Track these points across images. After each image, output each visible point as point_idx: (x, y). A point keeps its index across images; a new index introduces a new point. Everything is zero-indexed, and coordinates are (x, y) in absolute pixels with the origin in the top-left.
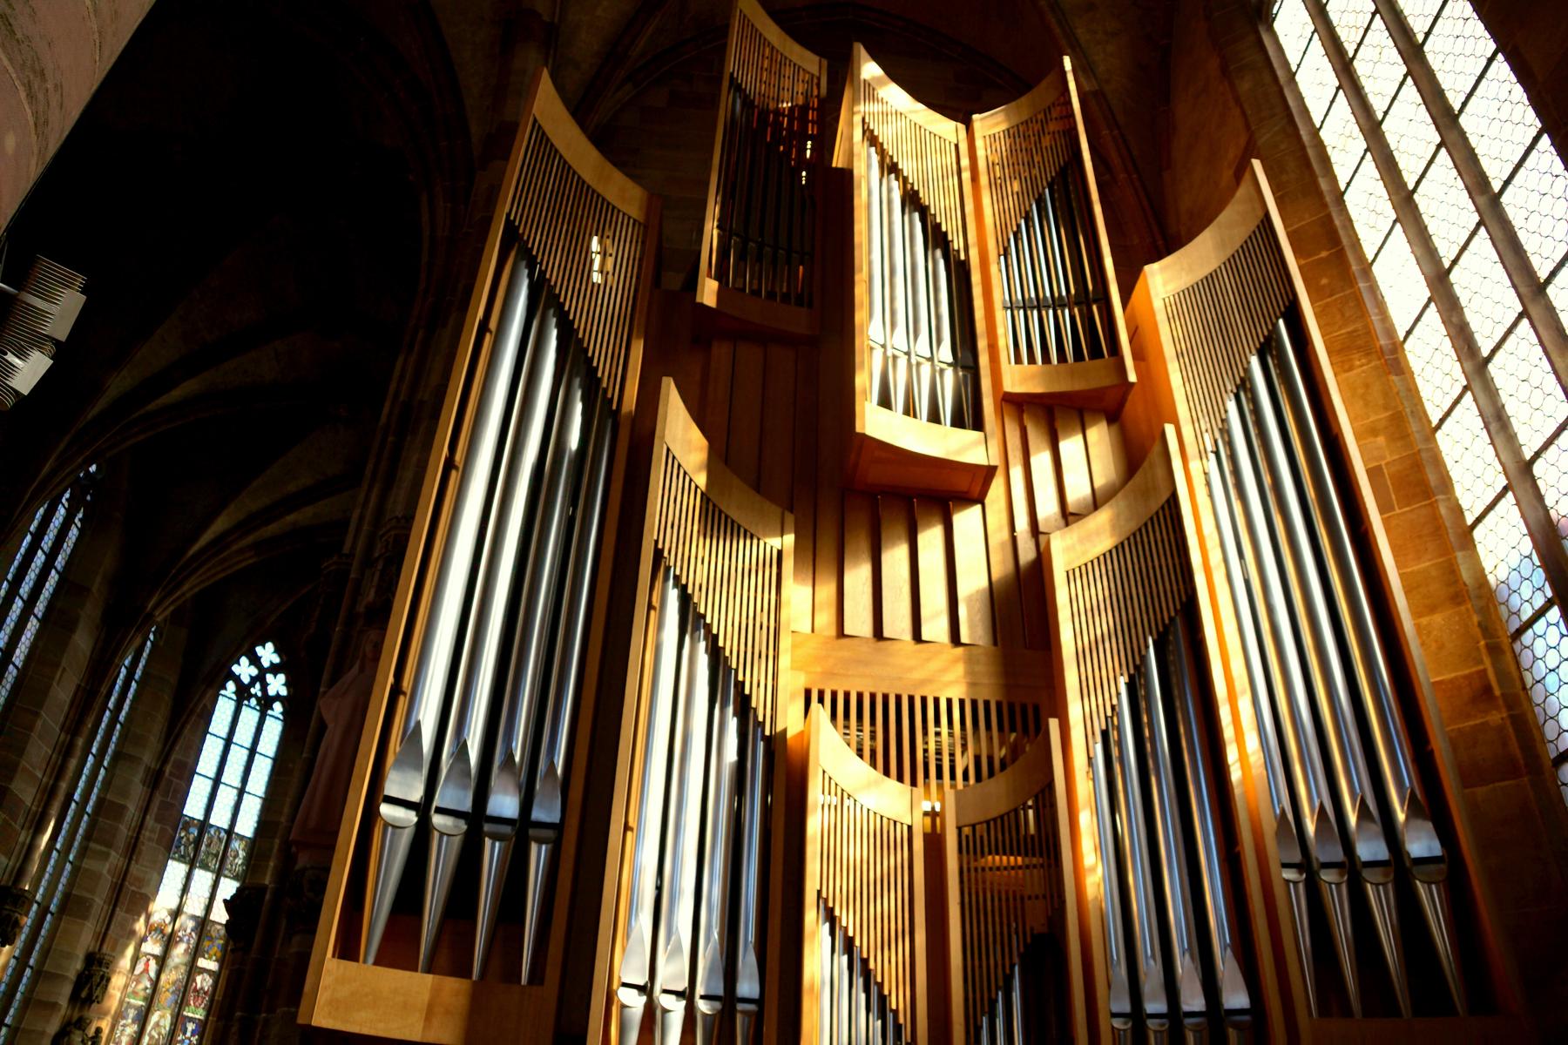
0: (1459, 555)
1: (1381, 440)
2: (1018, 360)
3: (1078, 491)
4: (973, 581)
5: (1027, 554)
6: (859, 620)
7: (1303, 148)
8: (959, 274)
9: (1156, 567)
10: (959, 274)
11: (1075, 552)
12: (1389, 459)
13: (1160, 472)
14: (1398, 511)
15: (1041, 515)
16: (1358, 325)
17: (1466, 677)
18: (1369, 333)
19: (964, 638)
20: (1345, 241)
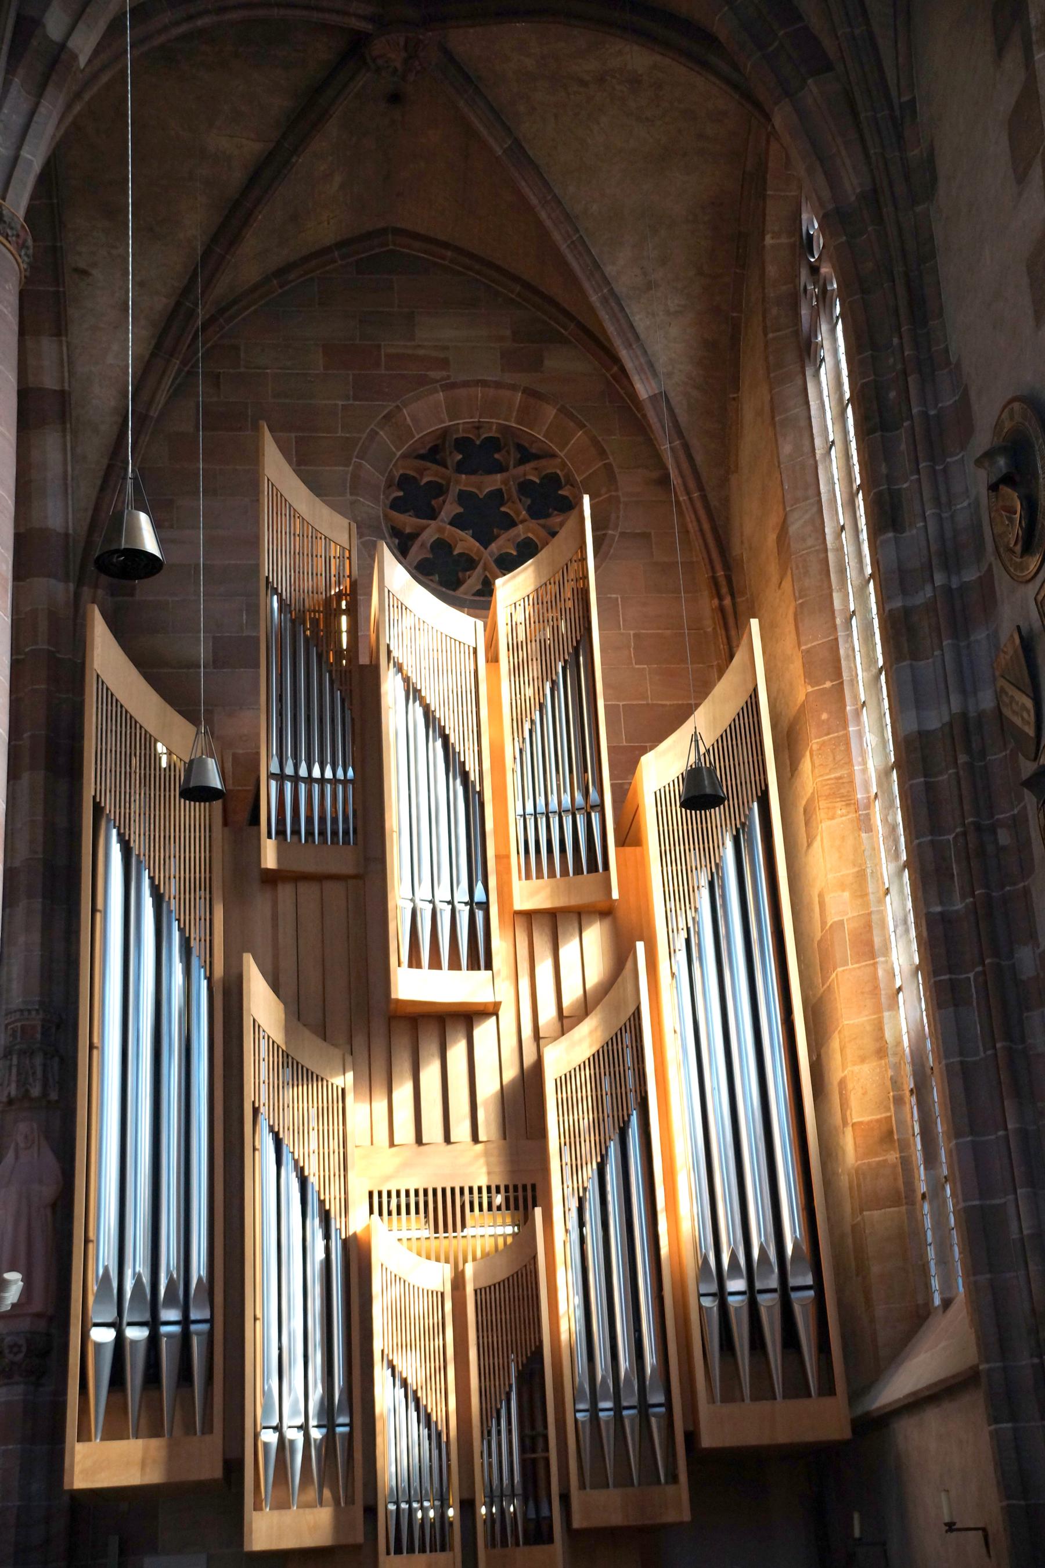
0: (886, 1014)
1: (846, 895)
2: (528, 877)
3: (572, 994)
4: (488, 1088)
5: (529, 1059)
6: (405, 1131)
7: (826, 550)
8: (474, 800)
9: (622, 1076)
10: (474, 800)
11: (568, 1056)
12: (850, 915)
13: (630, 987)
14: (850, 966)
15: (542, 1022)
16: (843, 772)
17: (878, 1121)
18: (852, 782)
19: (482, 1137)
20: (846, 676)
